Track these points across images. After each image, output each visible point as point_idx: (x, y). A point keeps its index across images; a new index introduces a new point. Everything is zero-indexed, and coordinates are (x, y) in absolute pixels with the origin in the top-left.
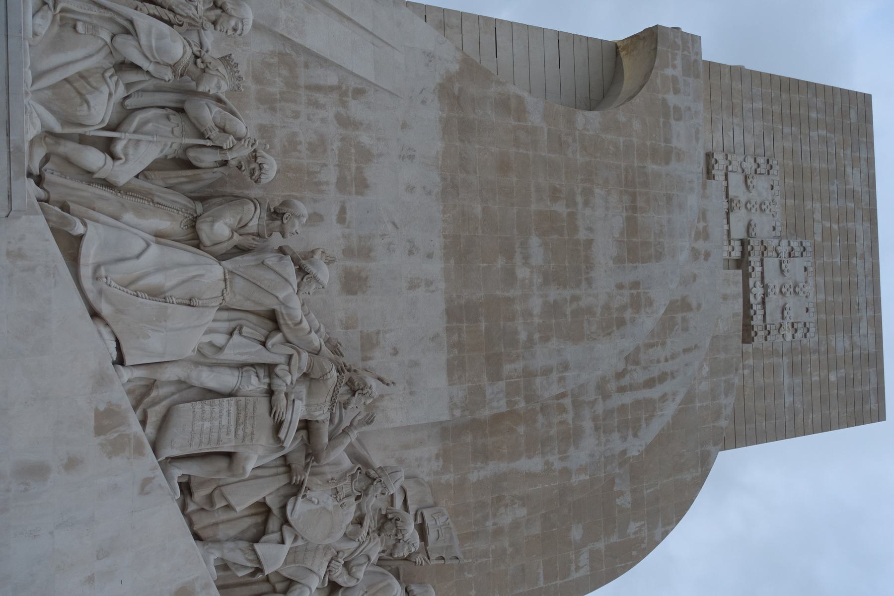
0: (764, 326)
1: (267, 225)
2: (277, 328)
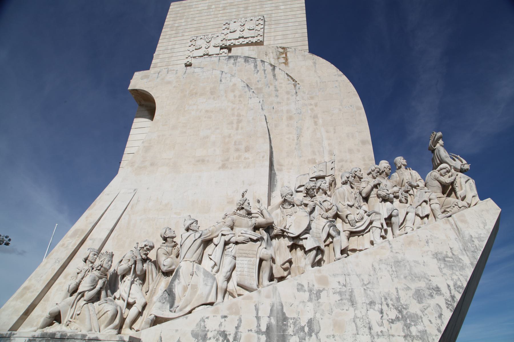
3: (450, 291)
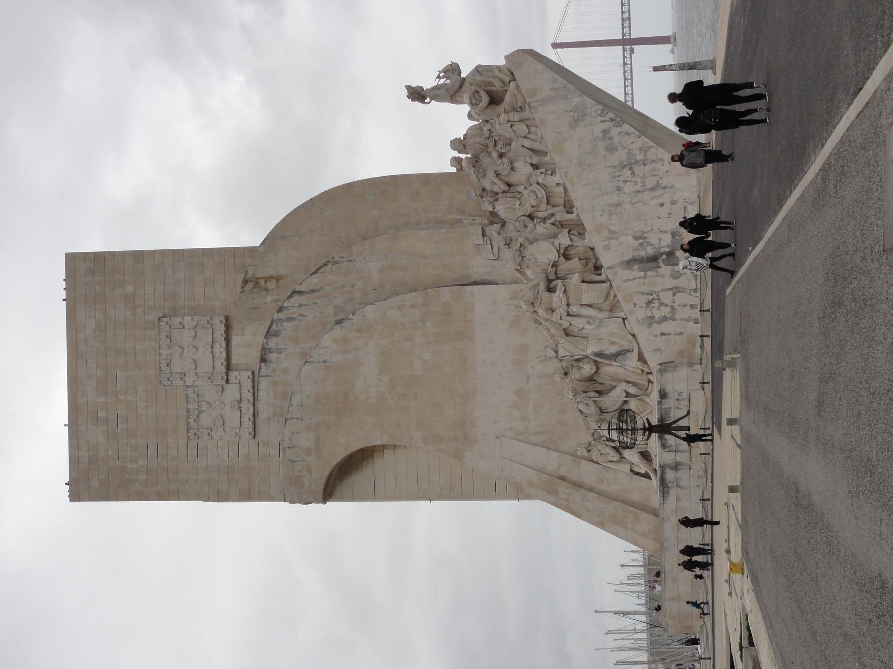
0: (213, 327)
1: (569, 370)
2: (564, 330)
3: (606, 121)
